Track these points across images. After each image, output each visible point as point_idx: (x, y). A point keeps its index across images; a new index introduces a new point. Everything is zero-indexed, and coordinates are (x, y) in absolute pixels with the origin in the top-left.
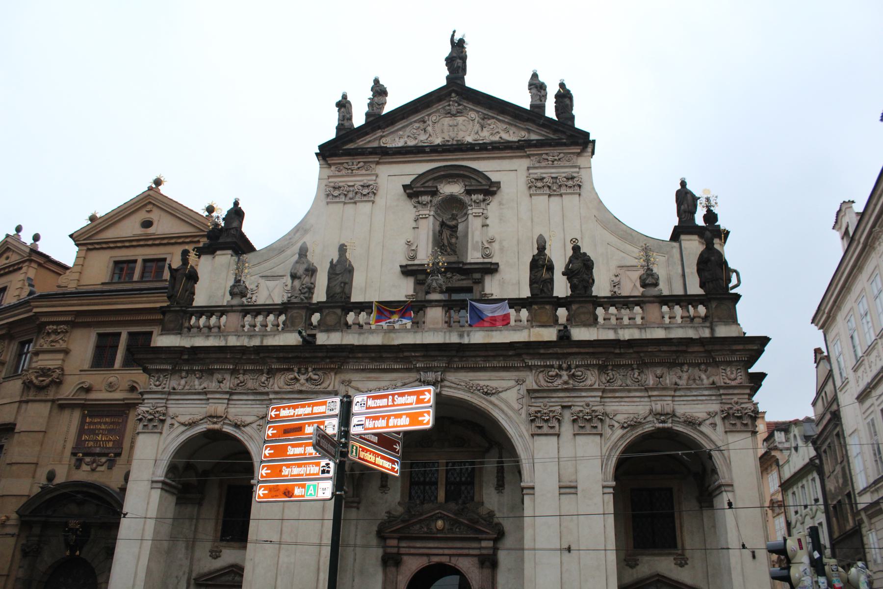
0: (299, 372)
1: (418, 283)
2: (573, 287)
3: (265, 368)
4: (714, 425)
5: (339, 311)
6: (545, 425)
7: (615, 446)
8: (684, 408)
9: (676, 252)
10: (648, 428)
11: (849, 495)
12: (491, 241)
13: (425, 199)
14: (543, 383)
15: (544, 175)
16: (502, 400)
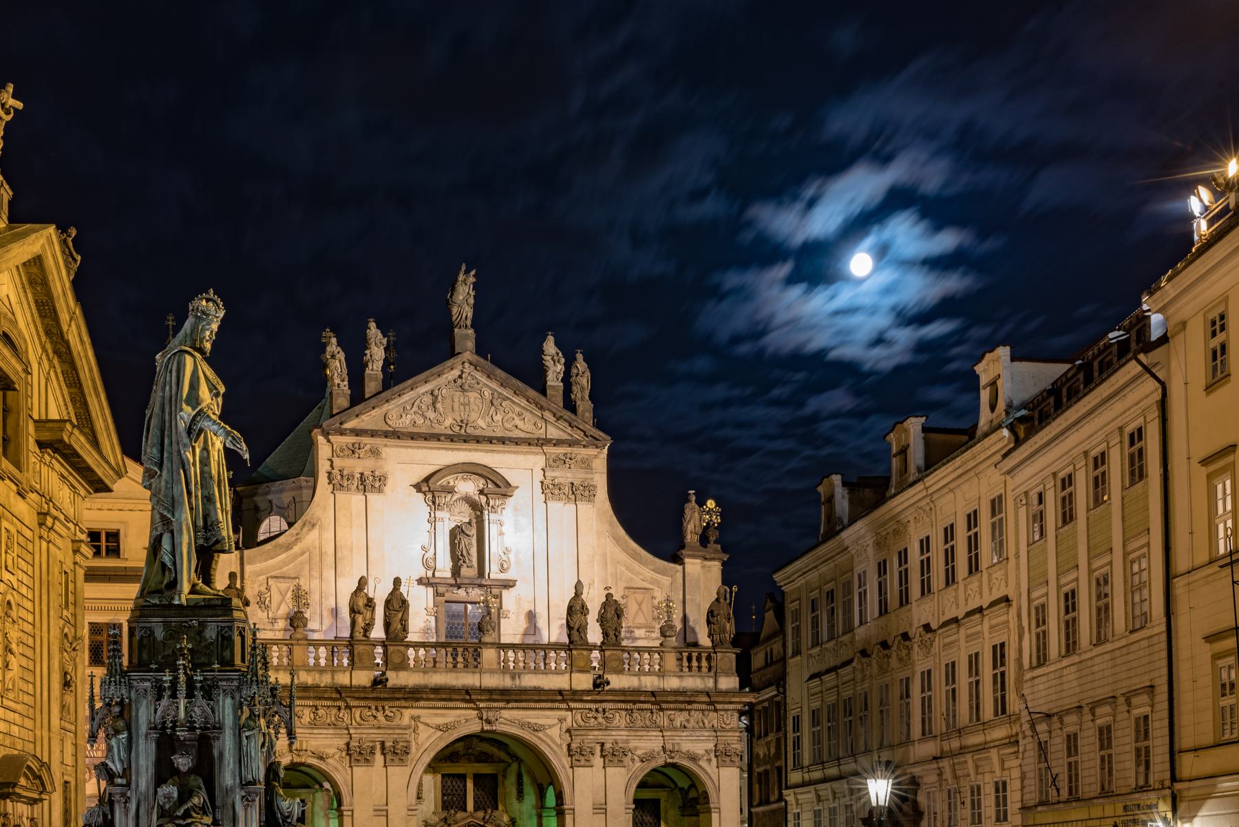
0: (377, 709)
1: (437, 594)
2: (605, 634)
3: (342, 704)
4: (709, 760)
5: (402, 648)
6: (582, 759)
7: (636, 777)
8: (687, 746)
9: (680, 575)
10: (661, 762)
11: (779, 769)
12: (507, 551)
13: (443, 499)
14: (582, 724)
15: (561, 480)
16: (548, 736)
